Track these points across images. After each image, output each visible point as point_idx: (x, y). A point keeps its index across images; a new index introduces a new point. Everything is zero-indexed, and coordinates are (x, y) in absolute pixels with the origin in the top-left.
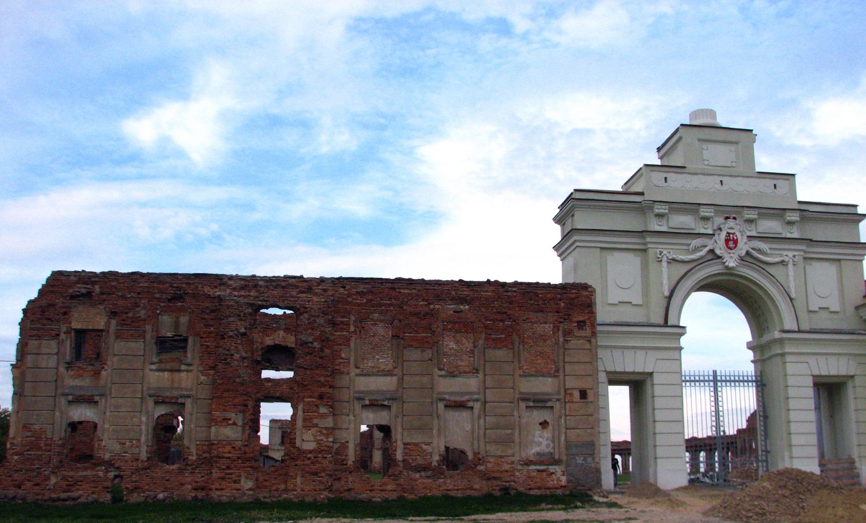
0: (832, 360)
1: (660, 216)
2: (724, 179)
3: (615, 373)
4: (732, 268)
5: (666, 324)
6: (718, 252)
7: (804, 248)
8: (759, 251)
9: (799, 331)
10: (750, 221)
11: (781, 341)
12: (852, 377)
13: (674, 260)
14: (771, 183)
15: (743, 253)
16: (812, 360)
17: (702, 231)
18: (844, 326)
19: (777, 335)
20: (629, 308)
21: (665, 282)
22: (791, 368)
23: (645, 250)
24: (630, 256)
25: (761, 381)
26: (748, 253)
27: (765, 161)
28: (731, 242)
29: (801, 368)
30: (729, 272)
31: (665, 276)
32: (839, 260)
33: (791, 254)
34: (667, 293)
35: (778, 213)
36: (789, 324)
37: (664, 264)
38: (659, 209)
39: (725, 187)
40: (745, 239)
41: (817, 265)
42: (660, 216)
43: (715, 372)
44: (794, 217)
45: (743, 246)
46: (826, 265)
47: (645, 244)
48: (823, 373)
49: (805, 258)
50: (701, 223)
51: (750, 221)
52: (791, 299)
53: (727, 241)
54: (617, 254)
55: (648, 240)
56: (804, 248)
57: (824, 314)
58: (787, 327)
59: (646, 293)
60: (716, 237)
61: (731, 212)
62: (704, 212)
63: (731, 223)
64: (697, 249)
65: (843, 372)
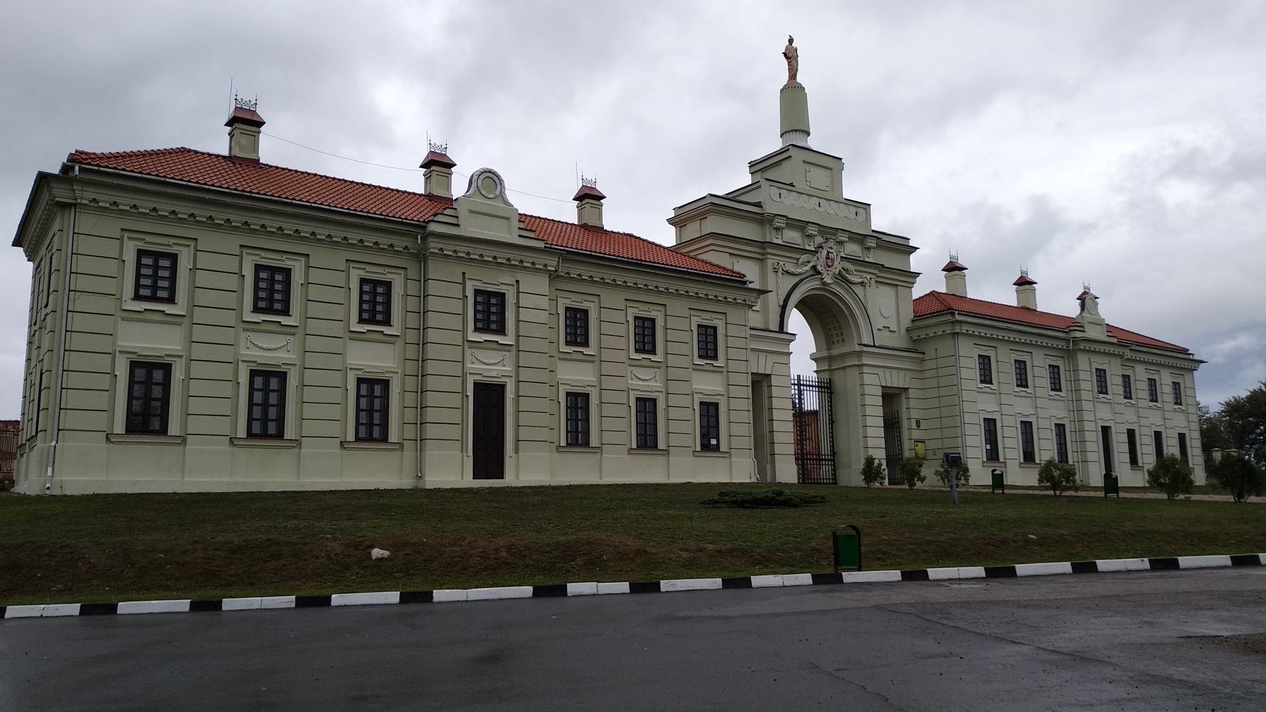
2: (822, 202)
8: (846, 270)
11: (859, 354)
12: (906, 389)
14: (853, 210)
16: (880, 371)
19: (857, 348)
22: (867, 379)
35: (859, 238)
38: (779, 223)
39: (822, 209)
45: (838, 266)
50: (806, 240)
55: (769, 251)
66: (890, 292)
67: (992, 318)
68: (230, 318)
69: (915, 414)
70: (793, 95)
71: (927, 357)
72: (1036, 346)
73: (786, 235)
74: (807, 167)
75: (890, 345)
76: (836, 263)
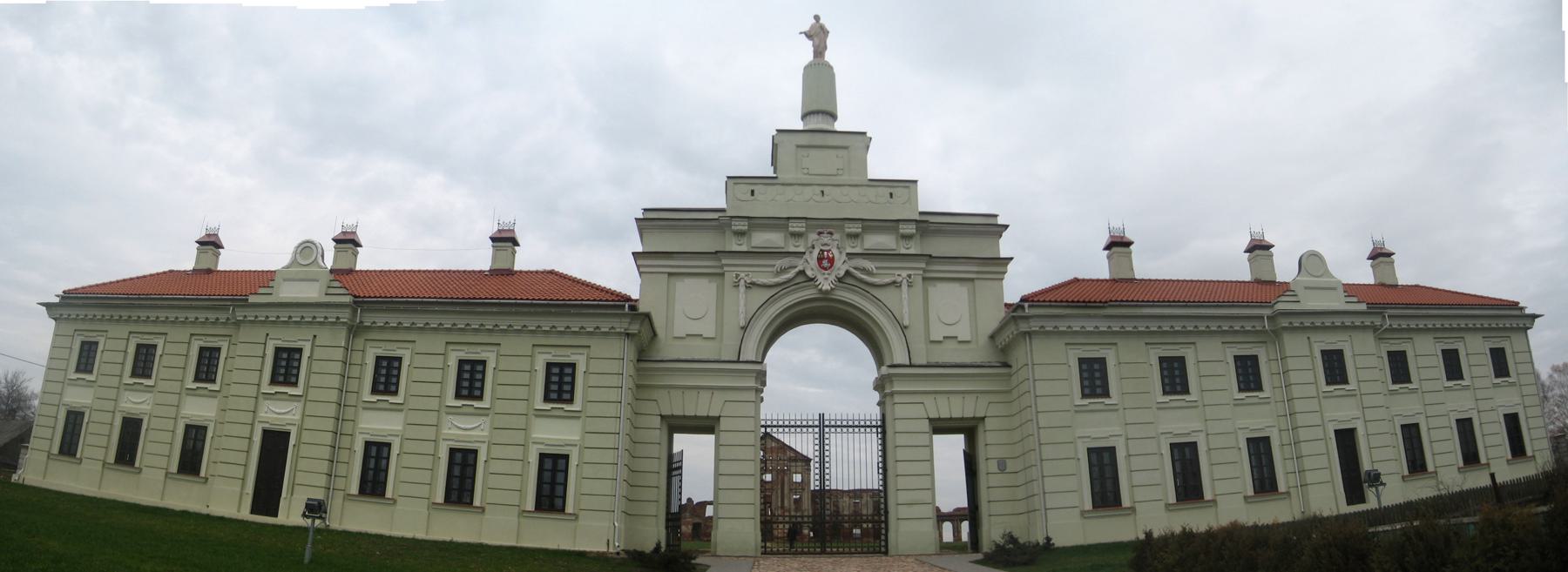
0: (970, 399)
1: (741, 234)
2: (826, 190)
3: (673, 416)
4: (827, 292)
5: (738, 361)
6: (809, 273)
7: (923, 265)
8: (864, 270)
9: (911, 366)
10: (855, 236)
12: (983, 419)
13: (753, 284)
15: (842, 273)
16: (928, 400)
17: (792, 249)
18: (978, 360)
20: (699, 342)
21: (742, 309)
23: (722, 275)
24: (704, 281)
25: (883, 426)
26: (847, 273)
27: (879, 166)
28: (826, 261)
29: (918, 411)
30: (825, 296)
31: (742, 302)
32: (972, 280)
33: (904, 274)
34: (742, 323)
35: (890, 226)
36: (900, 357)
37: (742, 289)
39: (826, 198)
40: (844, 257)
41: (941, 286)
42: (741, 234)
43: (821, 416)
44: (910, 229)
45: (841, 267)
46: (955, 286)
47: (722, 267)
48: (943, 416)
49: (924, 279)
51: (855, 236)
52: (904, 328)
53: (820, 260)
54: (689, 281)
56: (923, 265)
57: (951, 345)
58: (898, 361)
59: (720, 324)
60: (807, 256)
61: (824, 226)
62: (795, 227)
63: (826, 239)
64: (783, 271)
65: (969, 414)
66: (960, 292)
67: (1408, 306)
68: (434, 404)
69: (994, 452)
70: (819, 78)
71: (1014, 369)
72: (1467, 329)
73: (815, 236)
74: (804, 152)
75: (967, 360)
76: (838, 263)
